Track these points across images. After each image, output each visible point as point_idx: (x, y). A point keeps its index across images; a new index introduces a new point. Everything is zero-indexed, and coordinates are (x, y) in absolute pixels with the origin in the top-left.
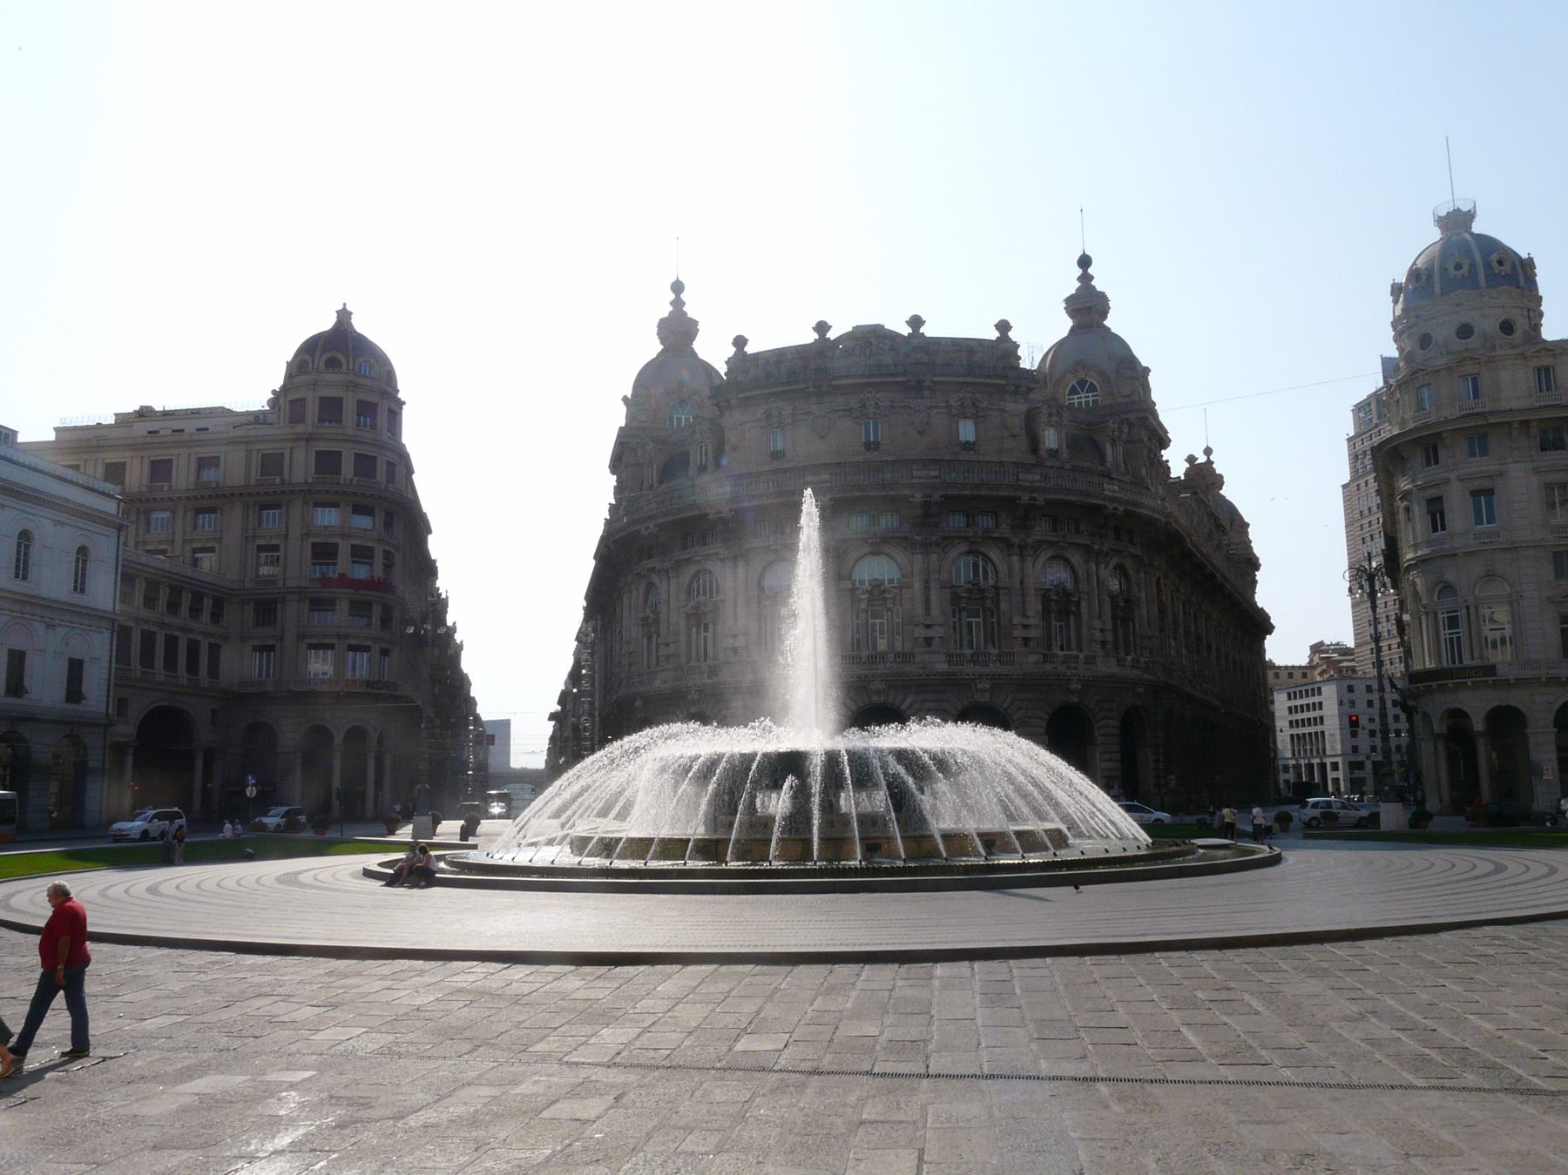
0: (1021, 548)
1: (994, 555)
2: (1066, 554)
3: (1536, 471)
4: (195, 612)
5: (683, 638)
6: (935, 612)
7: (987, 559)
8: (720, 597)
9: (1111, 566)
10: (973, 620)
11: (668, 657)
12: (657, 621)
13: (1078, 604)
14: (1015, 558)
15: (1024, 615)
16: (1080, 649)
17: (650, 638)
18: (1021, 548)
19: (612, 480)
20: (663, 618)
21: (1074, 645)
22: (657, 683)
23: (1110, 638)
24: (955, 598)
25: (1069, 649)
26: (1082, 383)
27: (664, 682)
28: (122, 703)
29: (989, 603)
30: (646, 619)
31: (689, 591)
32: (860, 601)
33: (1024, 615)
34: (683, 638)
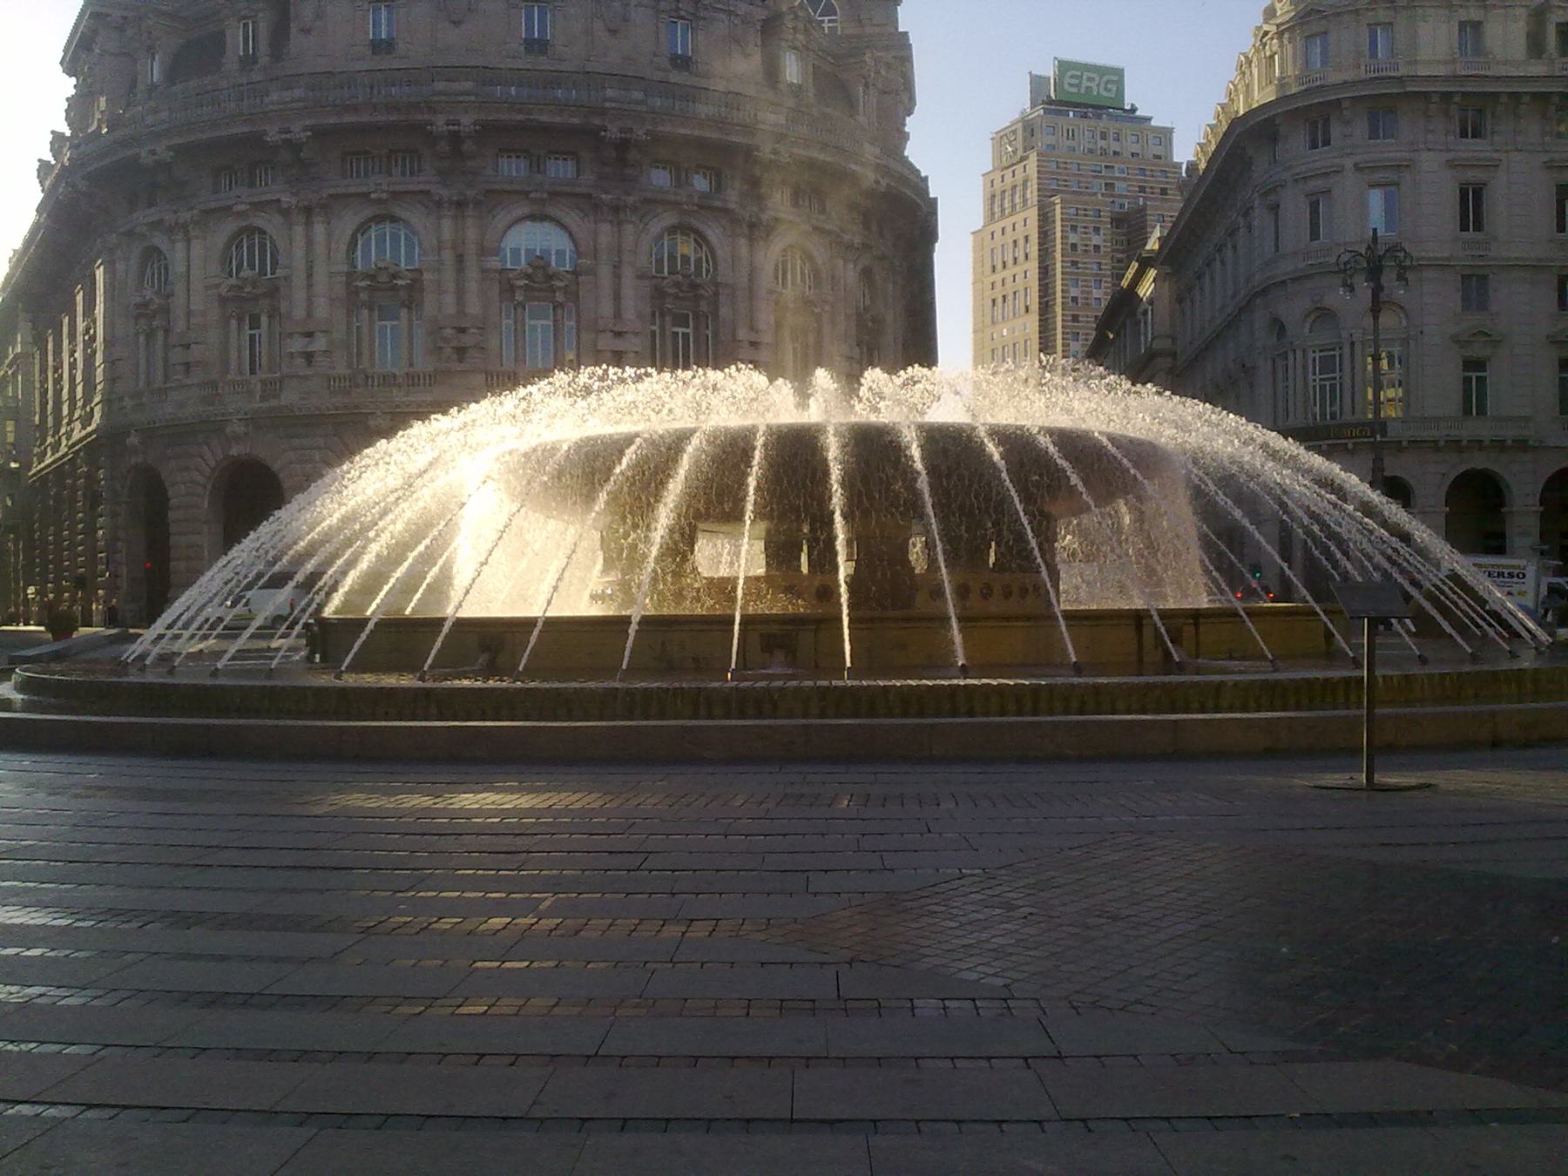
0: (752, 226)
1: (714, 234)
3: (1452, 165)
6: (629, 313)
7: (701, 239)
8: (280, 272)
10: (680, 330)
11: (187, 365)
12: (166, 311)
14: (743, 242)
17: (150, 335)
18: (752, 226)
19: (68, 86)
20: (179, 301)
24: (659, 293)
29: (704, 306)
30: (146, 305)
31: (226, 260)
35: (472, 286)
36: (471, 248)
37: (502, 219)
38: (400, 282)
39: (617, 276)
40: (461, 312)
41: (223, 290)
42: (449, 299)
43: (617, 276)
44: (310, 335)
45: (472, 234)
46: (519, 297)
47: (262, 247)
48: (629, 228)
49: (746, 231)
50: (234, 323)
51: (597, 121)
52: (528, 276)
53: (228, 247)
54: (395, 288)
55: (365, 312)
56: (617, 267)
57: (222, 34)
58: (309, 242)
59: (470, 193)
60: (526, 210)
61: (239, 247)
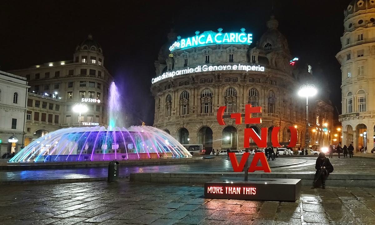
0: (243, 86)
1: (236, 88)
4: (51, 108)
5: (164, 111)
10: (230, 105)
14: (242, 90)
15: (243, 104)
22: (159, 122)
26: (268, 44)
27: (160, 122)
28: (29, 129)
33: (243, 104)
34: (164, 111)
35: (196, 101)
36: (196, 95)
37: (201, 90)
38: (186, 101)
40: (194, 105)
41: (165, 104)
42: (192, 104)
44: (174, 110)
45: (196, 93)
46: (203, 102)
48: (220, 89)
49: (242, 87)
50: (166, 109)
52: (205, 99)
54: (185, 102)
55: (181, 106)
58: (175, 96)
59: (196, 87)
60: (204, 88)
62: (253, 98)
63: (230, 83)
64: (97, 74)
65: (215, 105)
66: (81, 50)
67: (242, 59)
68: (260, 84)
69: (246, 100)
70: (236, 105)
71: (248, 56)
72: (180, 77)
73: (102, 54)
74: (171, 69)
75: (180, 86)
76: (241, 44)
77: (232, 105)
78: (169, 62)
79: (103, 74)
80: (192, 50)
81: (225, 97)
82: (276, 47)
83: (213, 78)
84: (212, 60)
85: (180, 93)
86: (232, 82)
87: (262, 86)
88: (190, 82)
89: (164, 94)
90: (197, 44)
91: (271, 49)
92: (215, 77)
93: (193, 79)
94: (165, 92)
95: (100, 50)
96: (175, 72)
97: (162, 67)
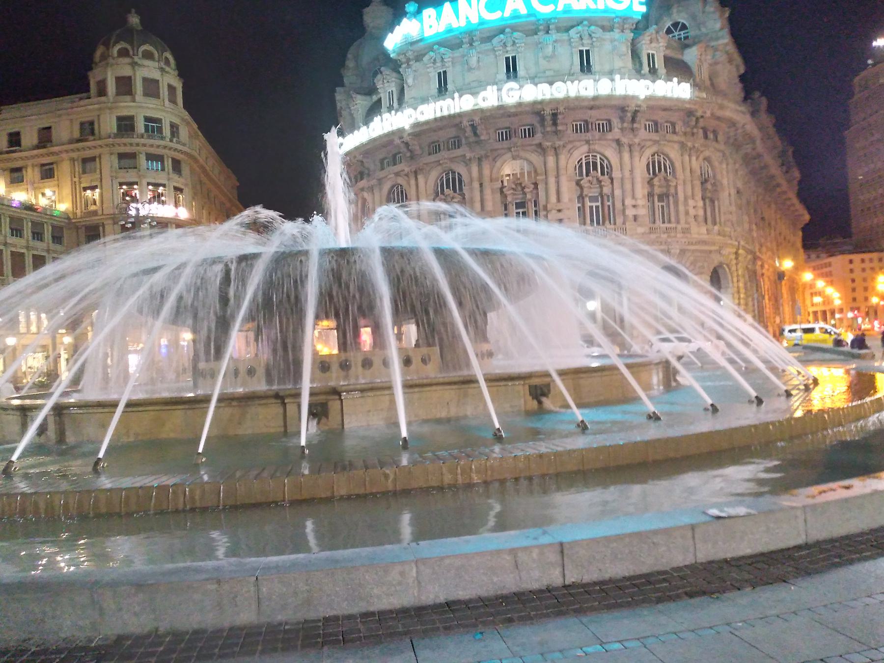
0: (630, 146)
2: (667, 150)
6: (565, 197)
9: (701, 158)
10: (594, 204)
13: (676, 187)
14: (626, 156)
15: (633, 197)
16: (678, 222)
21: (673, 219)
23: (701, 212)
25: (670, 222)
26: (676, 25)
29: (606, 190)
32: (506, 197)
33: (633, 197)
36: (486, 179)
39: (558, 183)
43: (558, 183)
45: (486, 172)
46: (509, 199)
47: (402, 192)
49: (627, 148)
51: (539, 107)
52: (513, 189)
53: (389, 193)
56: (557, 176)
57: (380, 100)
59: (483, 153)
61: (394, 193)
62: (660, 180)
63: (589, 136)
64: (167, 131)
65: (549, 206)
66: (111, 60)
67: (618, 64)
68: (675, 138)
69: (643, 188)
70: (610, 203)
71: (635, 54)
72: (434, 125)
73: (176, 73)
74: (396, 105)
75: (430, 154)
76: (614, 15)
77: (599, 204)
78: (386, 85)
79: (184, 132)
80: (458, 41)
81: (578, 183)
82: (704, 30)
83: (538, 125)
84: (527, 69)
85: (434, 175)
86: (597, 134)
87: (683, 145)
88: (464, 141)
89: (380, 181)
90: (475, 20)
91: (686, 38)
92: (542, 119)
93: (474, 128)
94: (381, 176)
95: (166, 58)
96: (415, 109)
97: (361, 103)
